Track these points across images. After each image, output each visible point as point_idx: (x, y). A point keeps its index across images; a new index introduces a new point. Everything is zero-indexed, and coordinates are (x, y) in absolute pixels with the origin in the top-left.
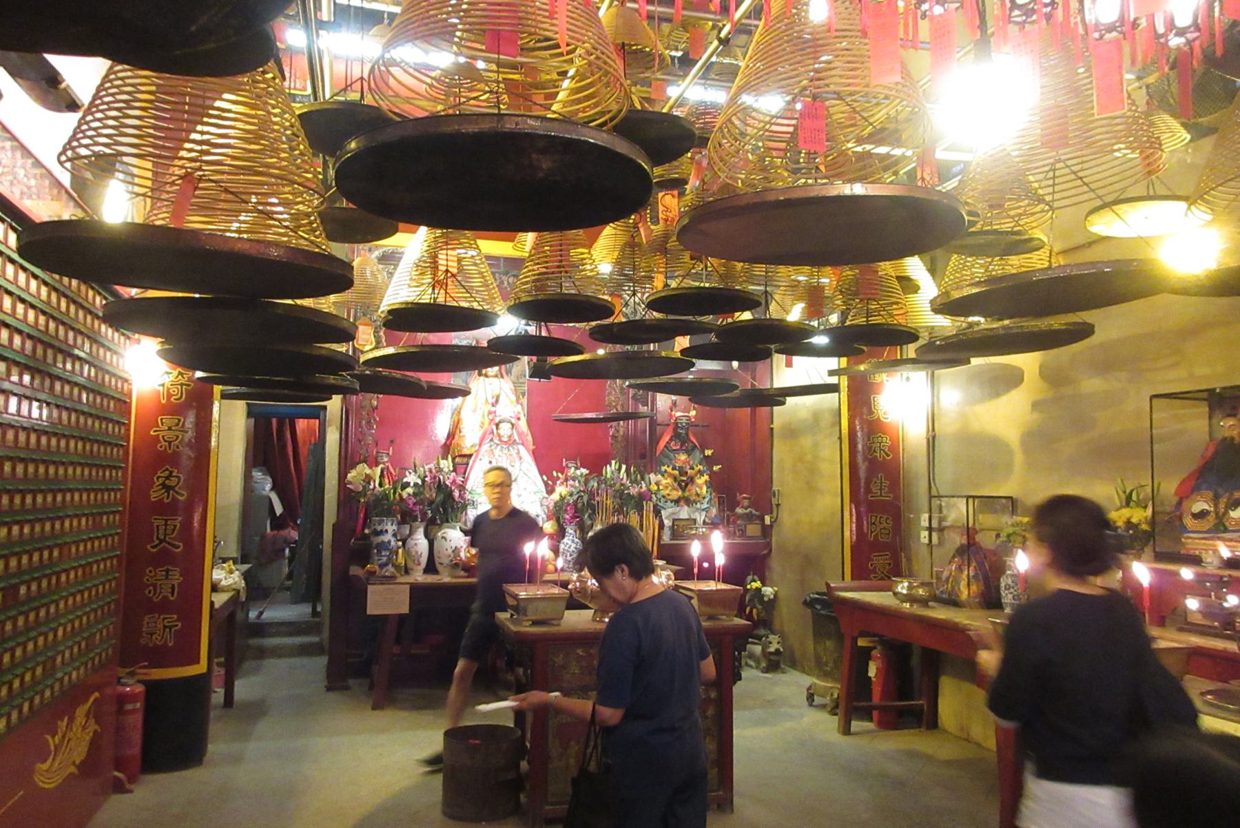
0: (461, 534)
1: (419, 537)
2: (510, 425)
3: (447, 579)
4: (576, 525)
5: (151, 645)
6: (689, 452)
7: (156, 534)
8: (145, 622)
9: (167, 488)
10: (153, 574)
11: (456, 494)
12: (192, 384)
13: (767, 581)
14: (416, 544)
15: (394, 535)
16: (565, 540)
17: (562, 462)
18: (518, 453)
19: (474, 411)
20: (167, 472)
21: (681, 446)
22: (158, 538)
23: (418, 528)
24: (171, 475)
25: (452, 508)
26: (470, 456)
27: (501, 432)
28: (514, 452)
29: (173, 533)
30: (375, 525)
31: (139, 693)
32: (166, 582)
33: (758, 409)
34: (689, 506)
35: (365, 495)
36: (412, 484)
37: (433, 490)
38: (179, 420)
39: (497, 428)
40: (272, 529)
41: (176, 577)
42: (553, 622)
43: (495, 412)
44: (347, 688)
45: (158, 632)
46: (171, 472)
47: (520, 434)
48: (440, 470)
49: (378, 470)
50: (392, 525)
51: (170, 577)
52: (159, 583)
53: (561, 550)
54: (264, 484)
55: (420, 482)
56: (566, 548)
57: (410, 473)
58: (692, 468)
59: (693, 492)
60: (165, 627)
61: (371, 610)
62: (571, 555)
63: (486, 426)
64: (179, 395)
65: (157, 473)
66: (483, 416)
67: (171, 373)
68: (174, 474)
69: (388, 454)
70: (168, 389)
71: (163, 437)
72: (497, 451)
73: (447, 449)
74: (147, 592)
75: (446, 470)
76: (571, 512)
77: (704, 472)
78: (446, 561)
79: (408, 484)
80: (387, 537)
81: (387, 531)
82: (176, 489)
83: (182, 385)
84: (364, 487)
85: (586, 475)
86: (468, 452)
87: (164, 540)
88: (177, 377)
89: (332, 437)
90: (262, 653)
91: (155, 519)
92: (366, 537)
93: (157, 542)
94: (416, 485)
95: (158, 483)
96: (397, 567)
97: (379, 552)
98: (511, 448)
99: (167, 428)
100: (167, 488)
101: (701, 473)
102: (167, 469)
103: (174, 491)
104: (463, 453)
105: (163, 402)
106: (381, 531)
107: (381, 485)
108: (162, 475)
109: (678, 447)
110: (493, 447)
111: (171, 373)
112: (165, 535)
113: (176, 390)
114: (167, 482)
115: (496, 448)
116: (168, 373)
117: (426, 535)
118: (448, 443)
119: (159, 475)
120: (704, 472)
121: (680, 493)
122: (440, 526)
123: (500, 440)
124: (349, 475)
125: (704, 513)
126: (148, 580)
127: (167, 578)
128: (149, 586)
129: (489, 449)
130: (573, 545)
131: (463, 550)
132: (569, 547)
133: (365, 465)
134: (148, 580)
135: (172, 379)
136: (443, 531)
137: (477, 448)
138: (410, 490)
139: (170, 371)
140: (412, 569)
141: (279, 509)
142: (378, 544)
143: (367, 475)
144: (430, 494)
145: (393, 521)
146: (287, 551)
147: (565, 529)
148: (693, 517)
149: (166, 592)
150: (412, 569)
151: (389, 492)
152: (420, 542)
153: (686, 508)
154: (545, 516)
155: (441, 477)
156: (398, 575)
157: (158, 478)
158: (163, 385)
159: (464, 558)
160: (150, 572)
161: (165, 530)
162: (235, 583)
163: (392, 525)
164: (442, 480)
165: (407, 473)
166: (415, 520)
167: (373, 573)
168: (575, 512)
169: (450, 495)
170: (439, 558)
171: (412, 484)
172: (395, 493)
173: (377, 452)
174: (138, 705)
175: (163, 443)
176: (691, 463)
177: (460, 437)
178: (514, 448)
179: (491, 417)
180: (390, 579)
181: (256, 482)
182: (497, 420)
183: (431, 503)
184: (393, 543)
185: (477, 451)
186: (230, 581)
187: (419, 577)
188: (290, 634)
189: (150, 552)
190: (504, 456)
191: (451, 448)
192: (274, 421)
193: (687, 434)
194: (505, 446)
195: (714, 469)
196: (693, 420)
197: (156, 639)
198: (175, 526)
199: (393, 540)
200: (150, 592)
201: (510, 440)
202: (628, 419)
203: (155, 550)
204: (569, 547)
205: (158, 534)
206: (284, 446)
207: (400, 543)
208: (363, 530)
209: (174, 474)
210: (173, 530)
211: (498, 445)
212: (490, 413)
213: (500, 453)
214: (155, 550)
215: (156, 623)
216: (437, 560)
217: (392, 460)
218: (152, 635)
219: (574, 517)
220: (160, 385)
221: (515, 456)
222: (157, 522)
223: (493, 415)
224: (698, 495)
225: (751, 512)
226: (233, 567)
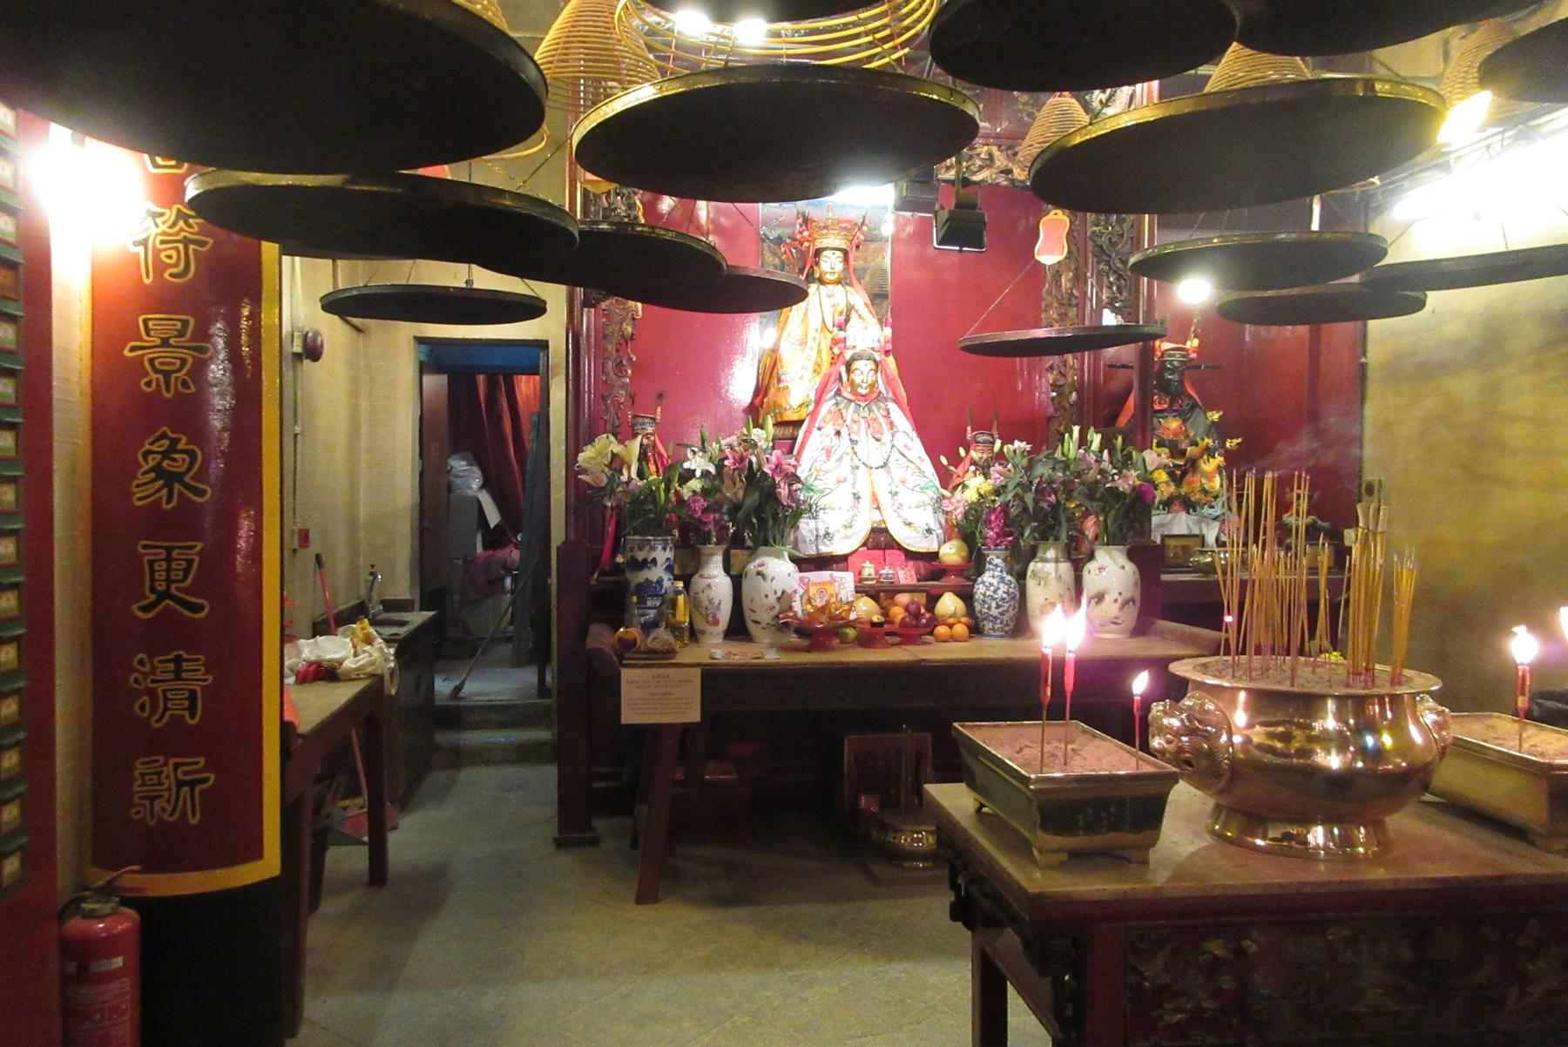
0: (791, 567)
1: (715, 572)
2: (871, 365)
3: (772, 657)
4: (1006, 549)
5: (152, 823)
6: (1184, 416)
7: (148, 583)
8: (137, 773)
9: (170, 478)
10: (147, 669)
11: (783, 491)
12: (211, 241)
13: (1339, 646)
14: (709, 586)
15: (669, 569)
16: (987, 577)
17: (965, 430)
18: (888, 415)
19: (803, 343)
20: (167, 442)
21: (1171, 405)
22: (153, 590)
23: (712, 555)
24: (173, 448)
25: (775, 516)
26: (799, 423)
27: (857, 377)
28: (878, 413)
29: (185, 577)
30: (632, 549)
31: (125, 932)
32: (178, 685)
33: (1325, 327)
34: (1189, 513)
35: (612, 491)
36: (698, 474)
37: (739, 484)
38: (185, 323)
39: (848, 371)
40: (485, 548)
41: (199, 675)
42: (1126, 853)
43: (844, 340)
44: (594, 842)
45: (166, 794)
46: (175, 441)
47: (888, 382)
48: (750, 444)
49: (635, 446)
50: (664, 549)
51: (184, 675)
52: (161, 687)
53: (978, 596)
54: (468, 477)
55: (712, 469)
56: (988, 593)
57: (694, 453)
58: (1195, 444)
59: (1197, 486)
60: (180, 784)
61: (629, 716)
62: (998, 607)
63: (825, 368)
64: (182, 265)
65: (143, 446)
66: (819, 352)
67: (161, 215)
68: (180, 446)
69: (654, 419)
70: (157, 252)
71: (151, 361)
72: (849, 413)
73: (754, 412)
74: (136, 707)
75: (762, 444)
76: (997, 522)
77: (1215, 449)
78: (766, 617)
79: (691, 473)
80: (657, 573)
81: (654, 561)
82: (187, 479)
83: (186, 242)
84: (611, 479)
85: (1029, 453)
86: (795, 417)
87: (166, 595)
88: (174, 224)
89: (558, 395)
90: (458, 758)
91: (145, 547)
92: (618, 570)
93: (153, 597)
94: (706, 474)
95: (146, 467)
96: (675, 629)
97: (642, 601)
98: (874, 408)
99: (158, 342)
100: (170, 478)
101: (1209, 452)
102: (164, 436)
103: (186, 486)
104: (786, 419)
105: (147, 281)
106: (645, 560)
107: (641, 475)
108: (154, 448)
109: (1166, 406)
110: (842, 406)
111: (161, 215)
112: (169, 581)
113: (174, 253)
114: (165, 464)
115: (847, 407)
116: (156, 215)
117: (727, 568)
118: (757, 402)
119: (148, 447)
120: (1215, 449)
121: (1172, 488)
122: (753, 552)
123: (854, 392)
124: (581, 456)
125: (1217, 524)
126: (136, 681)
127: (178, 678)
128: (140, 693)
129: (833, 408)
130: (1003, 588)
131: (797, 598)
132: (995, 592)
133: (612, 438)
134: (136, 681)
135: (163, 228)
136: (758, 561)
137: (811, 408)
138: (695, 484)
139: (160, 210)
140: (703, 632)
141: (493, 518)
142: (639, 585)
143: (614, 456)
144: (734, 491)
145: (665, 541)
146: (508, 581)
147: (985, 556)
148: (1196, 532)
149: (179, 706)
150: (703, 632)
151: (658, 488)
152: (716, 581)
153: (1183, 515)
154: (941, 531)
155: (754, 459)
156: (677, 645)
157: (146, 454)
158: (145, 243)
159: (800, 613)
160: (141, 662)
161: (169, 570)
162: (373, 663)
163: (664, 549)
164: (755, 466)
165: (690, 455)
166: (706, 540)
167: (629, 645)
168: (1006, 525)
169: (770, 494)
170: (754, 611)
171: (698, 474)
172: (667, 490)
173: (635, 417)
174: (118, 962)
175: (154, 376)
176: (1192, 434)
177: (779, 389)
178: (879, 408)
179: (836, 350)
180: (662, 656)
181: (456, 476)
182: (848, 355)
183: (736, 508)
184: (666, 584)
185: (814, 414)
186: (363, 659)
187: (717, 649)
188: (503, 725)
189: (136, 617)
190: (862, 421)
191: (762, 412)
192: (481, 378)
193: (1181, 382)
194: (863, 404)
195: (1228, 445)
196: (1194, 355)
197: (163, 810)
198: (190, 562)
199: (666, 577)
200: (142, 708)
201: (871, 392)
202: (1082, 350)
203: (150, 615)
204: (995, 592)
205: (153, 580)
206: (500, 419)
207: (680, 584)
208: (614, 555)
209: (180, 446)
210: (187, 572)
211: (851, 401)
212: (835, 342)
213: (855, 417)
214: (150, 615)
215: (159, 774)
216: (748, 615)
217: (661, 431)
218: (152, 799)
219: (1002, 534)
220: (137, 244)
221: (882, 420)
222: (148, 551)
223: (842, 345)
224: (1205, 492)
225: (1315, 522)
226: (371, 630)
